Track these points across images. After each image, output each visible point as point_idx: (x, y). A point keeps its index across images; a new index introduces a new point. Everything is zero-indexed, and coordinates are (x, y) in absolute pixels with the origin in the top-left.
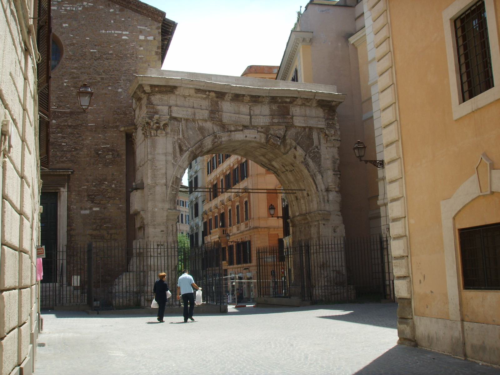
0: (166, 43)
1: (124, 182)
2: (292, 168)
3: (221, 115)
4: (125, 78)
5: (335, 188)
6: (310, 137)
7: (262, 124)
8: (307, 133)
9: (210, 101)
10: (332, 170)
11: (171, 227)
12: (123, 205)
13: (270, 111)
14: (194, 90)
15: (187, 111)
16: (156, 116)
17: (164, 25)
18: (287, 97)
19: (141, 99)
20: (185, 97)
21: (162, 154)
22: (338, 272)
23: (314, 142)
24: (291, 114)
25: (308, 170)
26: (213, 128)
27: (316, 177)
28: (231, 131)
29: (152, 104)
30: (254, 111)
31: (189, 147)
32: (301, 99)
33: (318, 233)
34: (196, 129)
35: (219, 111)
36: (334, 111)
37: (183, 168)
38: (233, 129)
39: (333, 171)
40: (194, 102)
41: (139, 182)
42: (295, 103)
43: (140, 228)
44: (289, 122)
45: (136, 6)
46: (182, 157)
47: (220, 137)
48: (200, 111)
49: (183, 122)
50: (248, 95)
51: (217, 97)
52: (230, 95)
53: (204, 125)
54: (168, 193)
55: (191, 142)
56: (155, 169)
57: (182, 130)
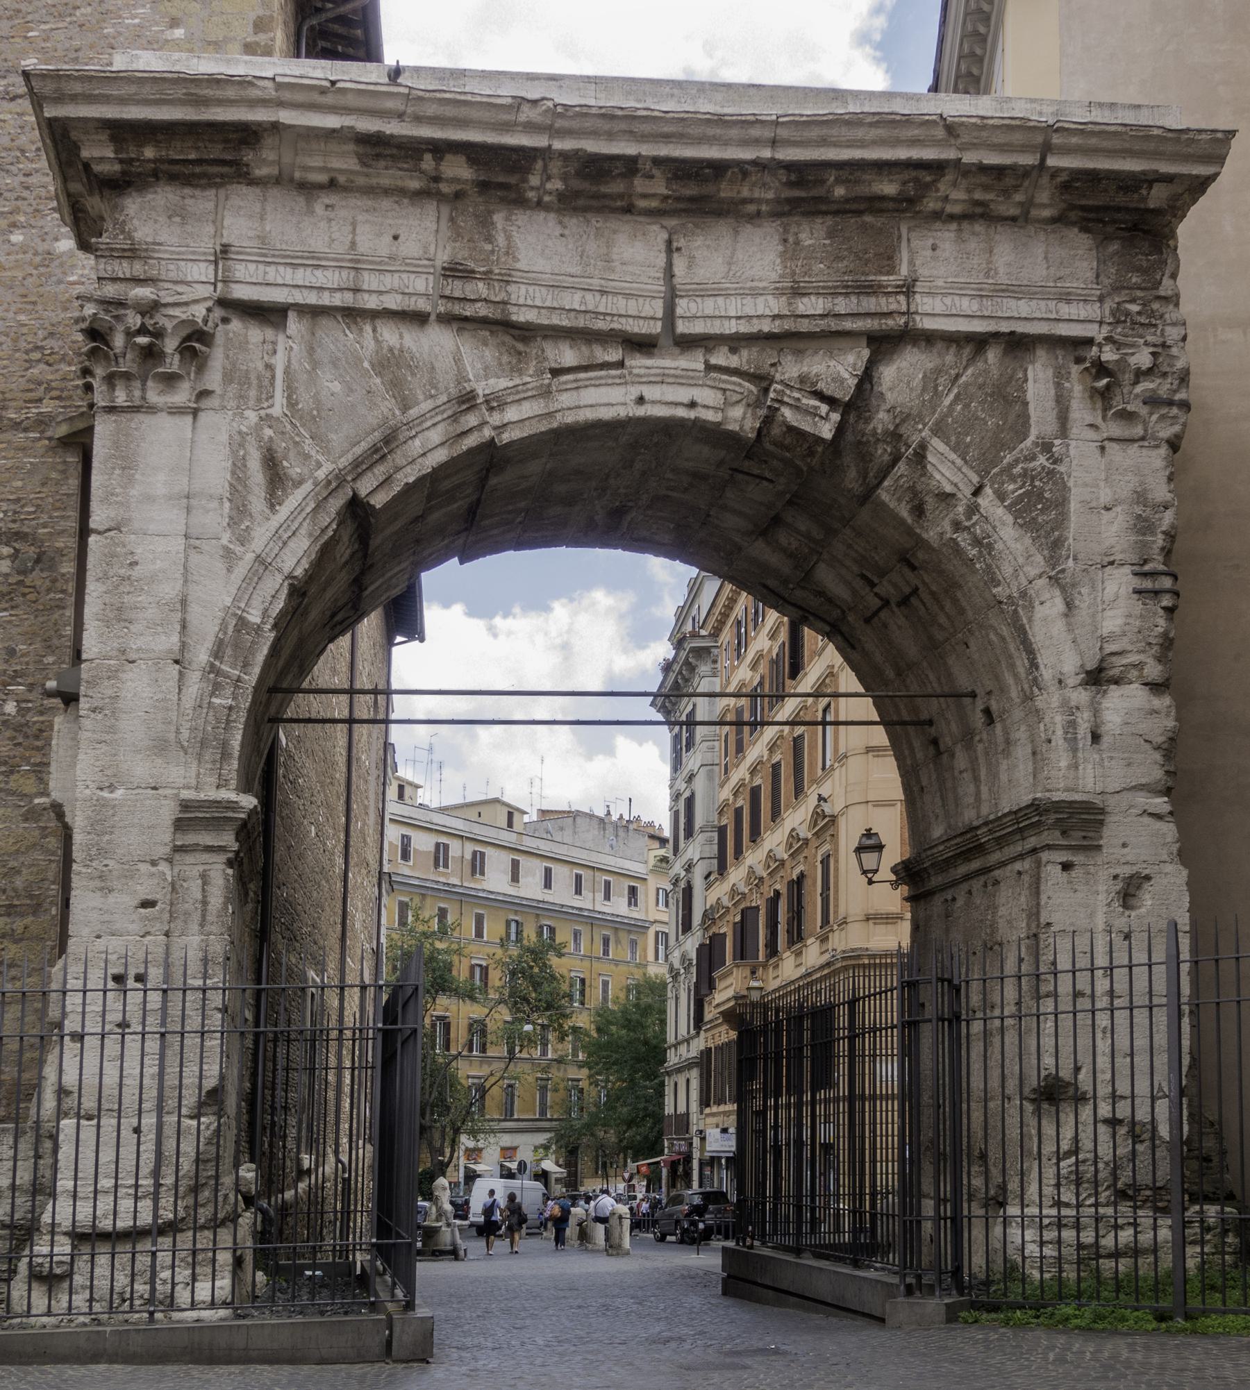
5: (1139, 666)
8: (995, 372)
10: (1127, 570)
11: (199, 882)
13: (782, 255)
21: (170, 498)
24: (904, 270)
26: (458, 360)
28: (556, 372)
31: (321, 458)
34: (366, 365)
37: (279, 570)
39: (1136, 574)
40: (360, 218)
42: (931, 205)
44: (889, 314)
55: (332, 436)
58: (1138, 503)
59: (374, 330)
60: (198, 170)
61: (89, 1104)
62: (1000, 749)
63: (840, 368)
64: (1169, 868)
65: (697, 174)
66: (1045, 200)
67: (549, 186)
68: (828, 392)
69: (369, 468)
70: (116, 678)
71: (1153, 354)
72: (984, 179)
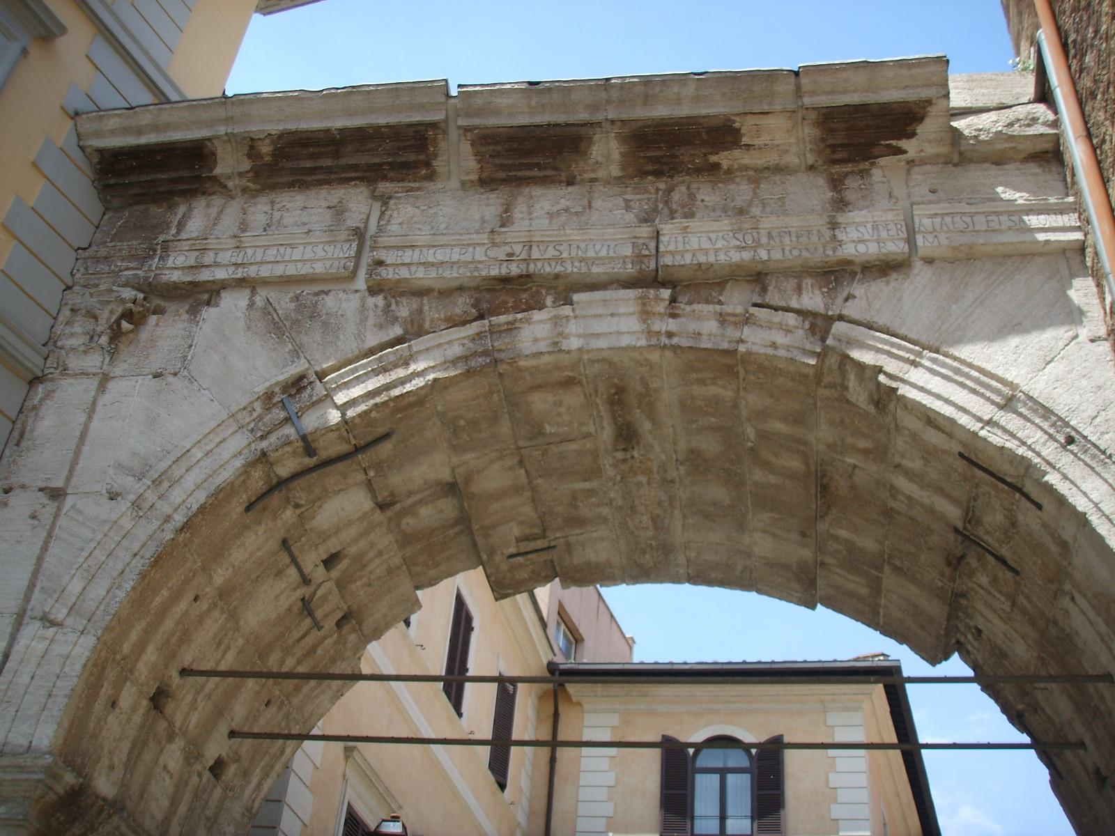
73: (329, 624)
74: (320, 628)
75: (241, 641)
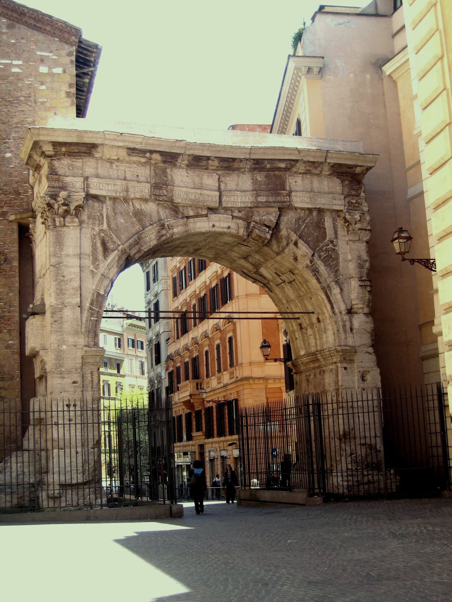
0: (87, 80)
1: (16, 303)
2: (292, 277)
3: (172, 191)
4: (16, 135)
5: (362, 308)
6: (320, 226)
7: (239, 205)
8: (316, 219)
9: (152, 168)
10: (357, 279)
11: (90, 375)
12: (14, 342)
13: (252, 183)
14: (125, 150)
15: (115, 185)
16: (63, 194)
17: (81, 50)
18: (280, 160)
19: (41, 167)
20: (110, 162)
21: (74, 255)
22: (371, 447)
23: (327, 234)
24: (288, 188)
25: (318, 279)
26: (158, 213)
27: (330, 290)
28: (188, 217)
29: (56, 174)
30: (226, 184)
31: (119, 243)
32: (304, 162)
33: (337, 382)
34: (131, 214)
35: (167, 185)
36: (359, 182)
37: (108, 277)
38: (191, 213)
39: (360, 281)
40: (127, 170)
41: (38, 303)
42: (294, 170)
43: (41, 378)
44: (285, 202)
45: (34, 19)
46: (106, 260)
47: (170, 227)
48: (136, 184)
49: (109, 203)
50: (216, 157)
51: (164, 162)
52: (186, 158)
53: (143, 207)
54: (84, 319)
55: (122, 236)
56: (62, 281)
57: (107, 216)
58: (359, 260)
59: (133, 204)
60: (78, 154)
61: (61, 444)
62: (323, 330)
63: (271, 217)
64: (374, 369)
65: (227, 160)
66: (326, 170)
67: (184, 163)
68: (267, 224)
69: (134, 246)
70: (61, 311)
71: (360, 216)
72: (310, 164)
73: (294, 277)
74: (295, 280)
75: (297, 301)
